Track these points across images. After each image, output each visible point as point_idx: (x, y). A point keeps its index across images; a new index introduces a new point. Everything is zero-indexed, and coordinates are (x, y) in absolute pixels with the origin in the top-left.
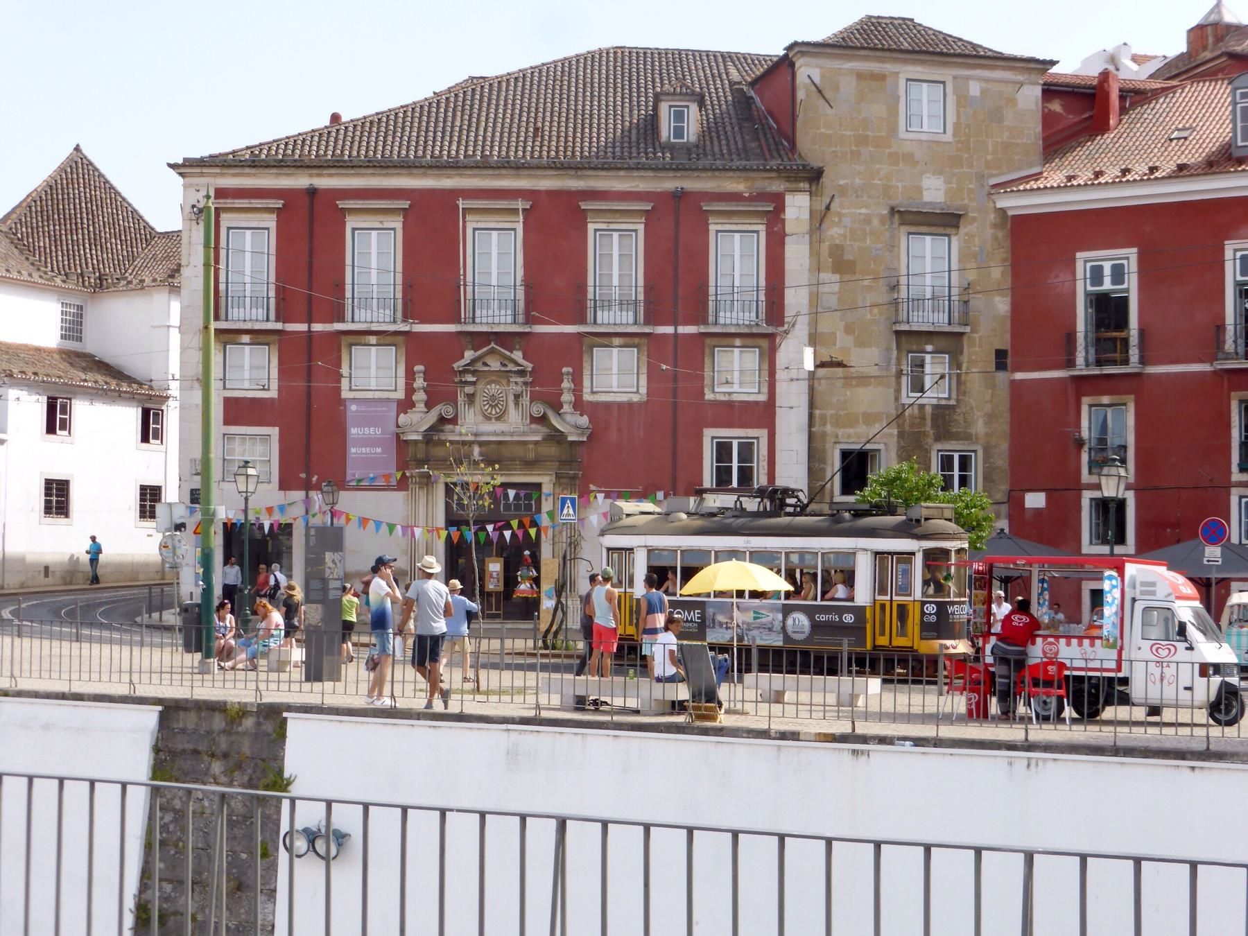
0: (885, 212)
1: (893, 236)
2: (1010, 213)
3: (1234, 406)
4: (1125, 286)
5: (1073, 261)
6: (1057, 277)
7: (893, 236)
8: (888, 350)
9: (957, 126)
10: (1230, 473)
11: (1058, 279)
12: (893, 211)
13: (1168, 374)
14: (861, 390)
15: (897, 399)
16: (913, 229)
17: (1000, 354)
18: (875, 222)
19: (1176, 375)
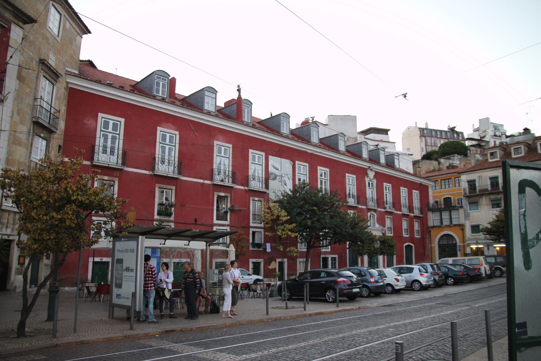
0: (38, 60)
1: (38, 74)
2: (70, 86)
3: (157, 189)
4: (118, 132)
5: (97, 116)
6: (88, 120)
7: (38, 74)
8: (30, 130)
9: (62, 36)
10: (153, 215)
11: (89, 122)
12: (40, 60)
13: (132, 172)
14: (19, 148)
15: (30, 157)
16: (45, 75)
17: (60, 146)
18: (34, 63)
19: (136, 173)
